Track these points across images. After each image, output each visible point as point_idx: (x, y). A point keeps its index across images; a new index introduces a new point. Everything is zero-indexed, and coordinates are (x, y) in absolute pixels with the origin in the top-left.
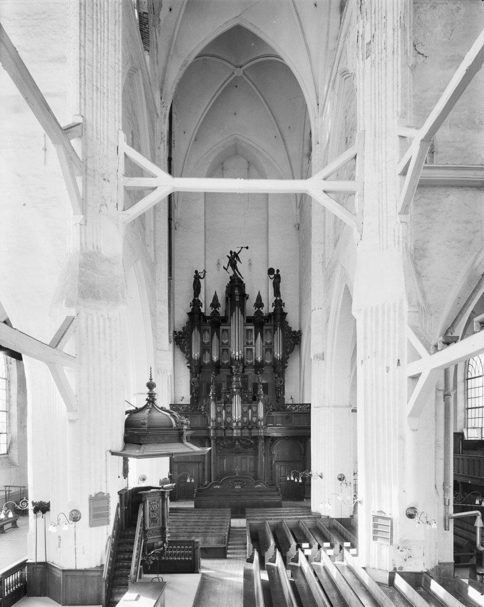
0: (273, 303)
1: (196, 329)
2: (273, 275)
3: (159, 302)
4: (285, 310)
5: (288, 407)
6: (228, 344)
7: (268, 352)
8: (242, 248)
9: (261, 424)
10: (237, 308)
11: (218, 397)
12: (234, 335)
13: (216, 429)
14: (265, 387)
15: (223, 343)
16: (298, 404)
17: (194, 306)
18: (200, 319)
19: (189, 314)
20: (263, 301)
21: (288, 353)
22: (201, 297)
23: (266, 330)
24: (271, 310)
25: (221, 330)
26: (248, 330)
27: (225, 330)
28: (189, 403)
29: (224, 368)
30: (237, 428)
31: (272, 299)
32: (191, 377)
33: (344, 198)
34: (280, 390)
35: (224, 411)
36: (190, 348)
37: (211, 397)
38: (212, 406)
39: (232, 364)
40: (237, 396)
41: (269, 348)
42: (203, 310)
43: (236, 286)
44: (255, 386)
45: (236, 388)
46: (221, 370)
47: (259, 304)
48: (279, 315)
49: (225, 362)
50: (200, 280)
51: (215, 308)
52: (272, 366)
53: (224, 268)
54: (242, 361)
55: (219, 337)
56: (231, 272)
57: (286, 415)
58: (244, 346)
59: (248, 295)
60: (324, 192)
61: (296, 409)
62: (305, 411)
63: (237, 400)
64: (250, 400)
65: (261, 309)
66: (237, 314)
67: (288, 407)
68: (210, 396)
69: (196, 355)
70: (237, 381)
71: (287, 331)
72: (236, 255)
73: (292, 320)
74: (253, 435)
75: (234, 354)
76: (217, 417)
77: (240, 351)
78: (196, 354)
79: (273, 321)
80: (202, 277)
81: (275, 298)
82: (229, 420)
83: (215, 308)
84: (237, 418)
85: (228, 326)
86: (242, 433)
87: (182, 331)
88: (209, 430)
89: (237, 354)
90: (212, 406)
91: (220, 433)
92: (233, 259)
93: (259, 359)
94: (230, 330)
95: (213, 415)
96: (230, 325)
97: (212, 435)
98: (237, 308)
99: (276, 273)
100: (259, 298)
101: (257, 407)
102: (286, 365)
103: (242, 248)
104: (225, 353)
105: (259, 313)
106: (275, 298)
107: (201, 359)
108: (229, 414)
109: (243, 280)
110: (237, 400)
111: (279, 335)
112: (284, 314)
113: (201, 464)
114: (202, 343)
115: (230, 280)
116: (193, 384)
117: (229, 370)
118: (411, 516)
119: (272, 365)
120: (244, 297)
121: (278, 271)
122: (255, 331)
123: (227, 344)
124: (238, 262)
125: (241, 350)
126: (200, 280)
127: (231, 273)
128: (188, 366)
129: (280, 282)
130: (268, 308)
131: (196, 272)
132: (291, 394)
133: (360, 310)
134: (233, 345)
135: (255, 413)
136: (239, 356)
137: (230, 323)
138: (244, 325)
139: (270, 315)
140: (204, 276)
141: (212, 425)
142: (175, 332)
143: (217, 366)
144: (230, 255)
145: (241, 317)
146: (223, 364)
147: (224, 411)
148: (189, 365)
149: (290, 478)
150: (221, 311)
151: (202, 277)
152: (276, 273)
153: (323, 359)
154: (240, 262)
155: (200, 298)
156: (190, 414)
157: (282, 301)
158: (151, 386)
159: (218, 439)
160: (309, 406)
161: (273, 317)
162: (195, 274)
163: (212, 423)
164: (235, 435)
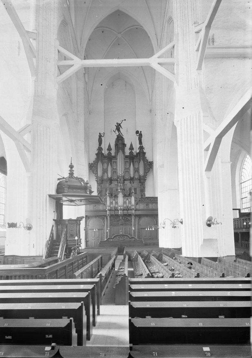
2: (139, 134)
3: (80, 141)
4: (145, 151)
6: (116, 169)
7: (137, 172)
10: (120, 150)
13: (110, 210)
14: (135, 189)
15: (114, 169)
18: (102, 156)
19: (96, 154)
20: (134, 147)
21: (146, 173)
22: (103, 146)
24: (138, 151)
25: (112, 162)
26: (126, 162)
27: (114, 162)
29: (114, 181)
30: (121, 209)
31: (138, 146)
32: (98, 186)
33: (170, 67)
34: (143, 191)
35: (114, 202)
36: (97, 171)
38: (108, 199)
39: (118, 178)
40: (120, 193)
41: (136, 170)
42: (103, 152)
43: (120, 141)
44: (130, 189)
45: (120, 189)
46: (112, 182)
47: (131, 148)
48: (142, 153)
50: (102, 137)
53: (114, 131)
54: (124, 177)
55: (111, 166)
56: (117, 133)
58: (124, 170)
60: (158, 64)
62: (155, 200)
63: (120, 196)
64: (127, 195)
65: (132, 151)
70: (121, 186)
73: (148, 157)
74: (129, 213)
78: (100, 173)
79: (139, 157)
80: (103, 136)
82: (116, 206)
83: (110, 151)
84: (121, 205)
85: (116, 160)
86: (123, 213)
87: (93, 163)
88: (106, 211)
90: (108, 199)
91: (113, 213)
95: (108, 203)
96: (117, 160)
98: (120, 150)
99: (140, 133)
100: (131, 145)
102: (146, 178)
104: (115, 173)
107: (102, 177)
108: (117, 203)
109: (123, 137)
111: (142, 164)
112: (145, 153)
114: (103, 168)
115: (117, 137)
117: (117, 182)
118: (209, 225)
119: (139, 178)
120: (124, 145)
121: (141, 132)
122: (130, 162)
123: (116, 169)
124: (121, 128)
127: (117, 133)
128: (96, 180)
130: (136, 150)
131: (100, 133)
132: (148, 194)
133: (178, 121)
134: (118, 169)
135: (130, 203)
138: (124, 159)
139: (137, 154)
142: (89, 163)
143: (111, 180)
144: (117, 125)
145: (122, 155)
147: (114, 202)
148: (96, 179)
149: (147, 229)
150: (113, 152)
151: (103, 136)
152: (140, 133)
153: (163, 167)
155: (102, 146)
158: (71, 167)
159: (111, 216)
160: (157, 198)
163: (108, 207)
164: (120, 213)
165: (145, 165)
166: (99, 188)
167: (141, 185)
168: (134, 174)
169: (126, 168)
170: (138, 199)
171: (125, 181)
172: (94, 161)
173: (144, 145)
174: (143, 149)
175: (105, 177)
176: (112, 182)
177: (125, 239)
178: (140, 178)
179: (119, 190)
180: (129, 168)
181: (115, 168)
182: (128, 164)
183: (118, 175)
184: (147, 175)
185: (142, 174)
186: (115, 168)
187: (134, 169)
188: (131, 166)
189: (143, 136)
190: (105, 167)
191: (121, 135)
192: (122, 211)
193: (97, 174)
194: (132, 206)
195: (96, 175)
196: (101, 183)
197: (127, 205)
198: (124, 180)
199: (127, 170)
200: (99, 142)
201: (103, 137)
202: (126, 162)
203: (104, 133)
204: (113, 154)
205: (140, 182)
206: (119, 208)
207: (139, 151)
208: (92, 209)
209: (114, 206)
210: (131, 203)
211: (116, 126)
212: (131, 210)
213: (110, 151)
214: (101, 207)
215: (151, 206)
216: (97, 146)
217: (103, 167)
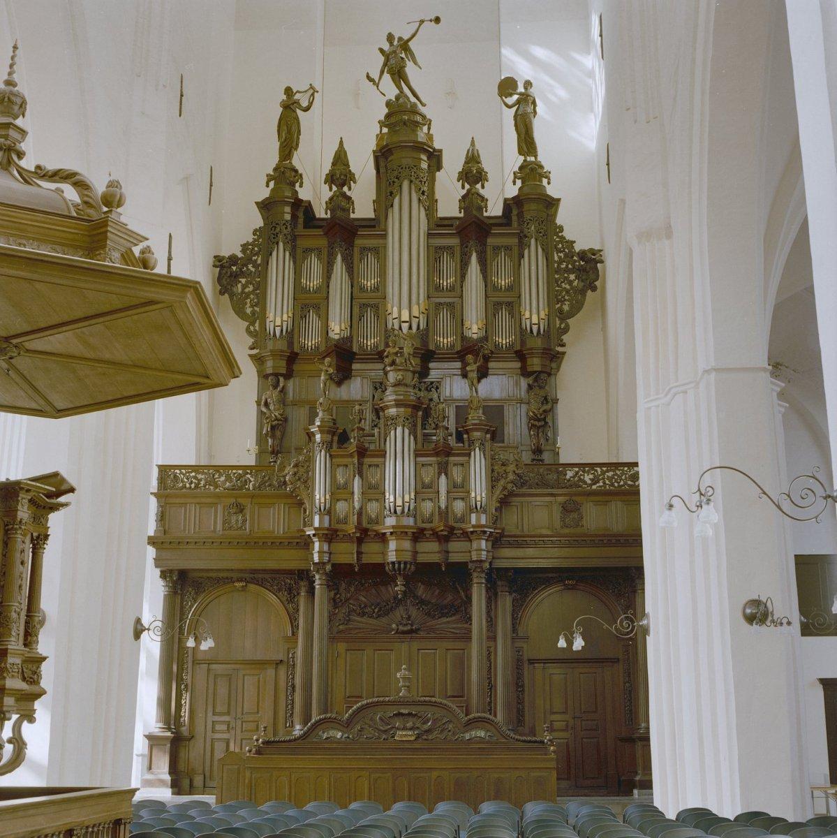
1: (281, 244)
2: (515, 97)
4: (552, 191)
5: (570, 474)
6: (380, 289)
7: (504, 314)
8: (422, 22)
9: (478, 519)
10: (406, 184)
11: (338, 437)
12: (397, 260)
13: (330, 535)
18: (294, 217)
19: (264, 206)
20: (486, 164)
21: (564, 316)
22: (299, 160)
23: (497, 249)
24: (512, 191)
25: (356, 250)
26: (440, 249)
27: (370, 249)
28: (253, 463)
30: (399, 532)
31: (514, 160)
34: (542, 422)
36: (261, 301)
37: (318, 437)
38: (320, 461)
40: (399, 430)
42: (304, 194)
45: (398, 404)
47: (473, 174)
49: (371, 342)
50: (298, 111)
52: (516, 352)
54: (424, 335)
55: (350, 270)
56: (389, 89)
57: (561, 499)
59: (441, 151)
61: (595, 481)
66: (407, 201)
67: (570, 474)
68: (313, 434)
69: (278, 322)
71: (559, 251)
74: (454, 558)
75: (395, 315)
76: (335, 498)
78: (278, 316)
80: (305, 104)
84: (399, 502)
86: (415, 553)
87: (240, 255)
88: (306, 544)
90: (320, 461)
91: (346, 554)
93: (475, 328)
94: (385, 247)
95: (320, 494)
96: (384, 236)
97: (316, 559)
99: (521, 89)
100: (473, 158)
101: (465, 466)
102: (560, 349)
103: (422, 22)
104: (369, 314)
105: (472, 202)
107: (290, 336)
108: (374, 491)
110: (399, 441)
112: (553, 204)
113: (282, 671)
114: (299, 290)
116: (264, 409)
121: (528, 84)
125: (418, 304)
126: (298, 111)
128: (250, 356)
131: (288, 91)
134: (392, 290)
135: (460, 489)
136: (410, 322)
137: (385, 230)
139: (509, 205)
140: (311, 104)
141: (317, 524)
142: (218, 259)
144: (386, 47)
146: (361, 347)
151: (305, 104)
152: (521, 89)
154: (415, 63)
156: (253, 497)
159: (339, 574)
161: (515, 212)
162: (284, 97)
163: (317, 518)
164: (392, 557)
166: (266, 404)
167: (530, 387)
168: (489, 326)
169: (438, 288)
170: (511, 468)
171: (431, 365)
172: (245, 247)
173: (546, 156)
174: (545, 181)
175: (311, 340)
176: (355, 366)
177: (428, 731)
178: (523, 343)
179: (393, 411)
180: (458, 290)
181: (370, 283)
182: (449, 266)
183: (390, 326)
184: (566, 330)
185: (535, 320)
186: (370, 283)
187: (489, 287)
190: (313, 280)
192: (407, 545)
193: (263, 317)
194: (472, 509)
195: (253, 323)
196: (284, 371)
197: (443, 506)
198: (427, 355)
201: (307, 109)
202: (435, 255)
203: (313, 91)
204: (363, 208)
206: (390, 521)
207: (520, 189)
208: (219, 527)
209: (357, 505)
210: (469, 492)
211: (381, 50)
212: (467, 536)
213: (345, 189)
214: (275, 521)
215: (594, 518)
216: (272, 159)
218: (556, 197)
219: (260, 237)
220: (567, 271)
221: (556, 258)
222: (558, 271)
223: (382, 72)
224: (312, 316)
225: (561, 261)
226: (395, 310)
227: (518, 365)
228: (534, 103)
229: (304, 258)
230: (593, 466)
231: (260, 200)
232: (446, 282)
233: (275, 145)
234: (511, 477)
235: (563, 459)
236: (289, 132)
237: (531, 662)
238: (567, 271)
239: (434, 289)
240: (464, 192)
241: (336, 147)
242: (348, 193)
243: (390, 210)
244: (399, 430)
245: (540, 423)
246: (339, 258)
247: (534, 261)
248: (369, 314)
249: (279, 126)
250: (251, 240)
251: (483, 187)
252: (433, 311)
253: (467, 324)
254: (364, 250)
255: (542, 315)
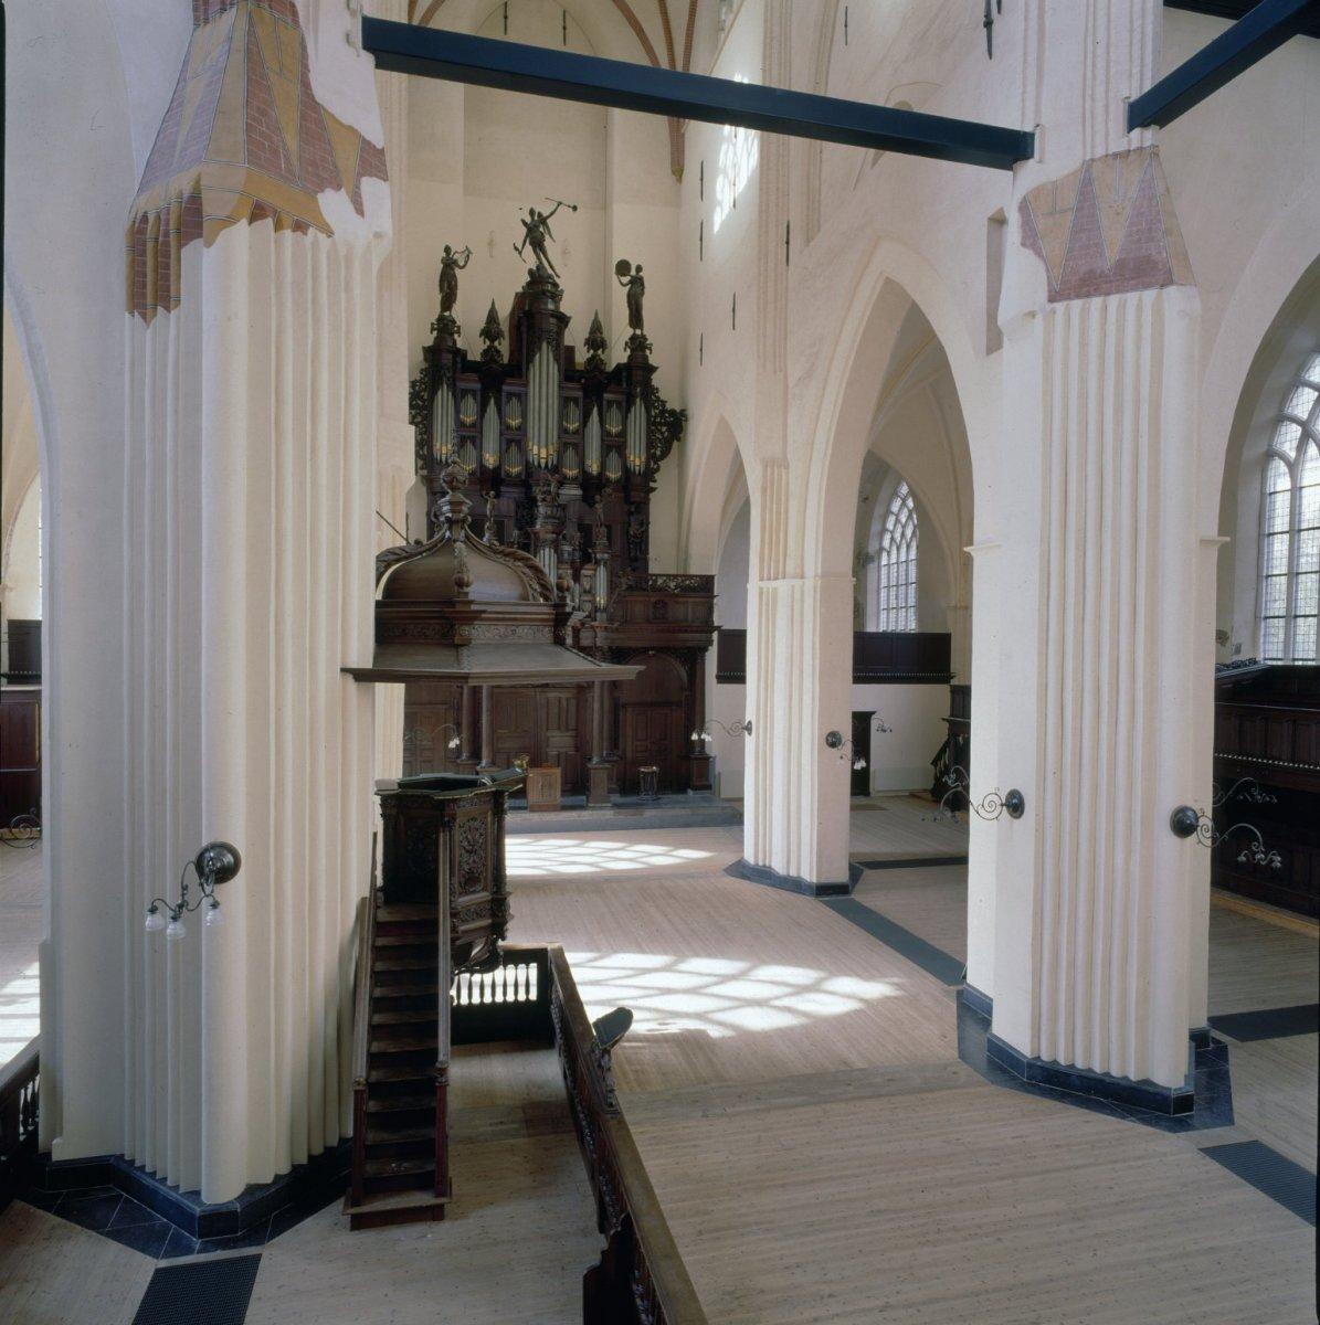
0: (626, 344)
1: (445, 386)
4: (653, 360)
5: (660, 581)
6: (522, 428)
8: (560, 204)
10: (544, 345)
15: (509, 427)
16: (681, 576)
17: (439, 330)
18: (455, 362)
21: (657, 459)
22: (458, 312)
23: (610, 403)
27: (514, 394)
40: (547, 550)
41: (614, 445)
47: (596, 341)
49: (515, 470)
50: (457, 271)
51: (492, 341)
53: (516, 249)
55: (499, 411)
65: (600, 352)
67: (660, 581)
71: (655, 408)
72: (543, 220)
77: (550, 447)
80: (462, 264)
81: (630, 332)
83: (492, 341)
89: (543, 454)
92: (536, 233)
96: (526, 385)
99: (633, 272)
100: (596, 328)
102: (652, 484)
104: (514, 448)
105: (595, 363)
106: (630, 332)
114: (460, 425)
116: (434, 519)
121: (639, 269)
124: (547, 237)
127: (532, 262)
129: (642, 294)
130: (618, 355)
131: (447, 250)
132: (661, 561)
134: (532, 431)
136: (547, 458)
140: (466, 262)
144: (528, 220)
146: (508, 475)
151: (462, 264)
152: (633, 272)
154: (551, 236)
157: (646, 339)
162: (444, 255)
165: (651, 423)
168: (603, 466)
169: (566, 431)
173: (650, 329)
174: (648, 352)
181: (514, 423)
182: (575, 412)
184: (658, 469)
185: (637, 463)
186: (514, 423)
188: (589, 424)
189: (646, 290)
190: (469, 418)
191: (550, 271)
199: (571, 442)
200: (441, 290)
202: (565, 402)
203: (468, 254)
205: (627, 500)
217: (457, 411)
218: (655, 365)
219: (425, 376)
220: (660, 424)
221: (653, 414)
222: (654, 424)
223: (525, 242)
224: (469, 445)
225: (655, 417)
226: (535, 448)
227: (623, 495)
228: (642, 284)
229: (463, 397)
230: (675, 576)
231: (426, 345)
232: (572, 427)
233: (438, 297)
234: (624, 587)
235: (650, 572)
236: (449, 287)
237: (624, 706)
238: (660, 424)
239: (563, 431)
240: (589, 355)
241: (489, 307)
242: (499, 347)
243: (531, 366)
244: (547, 550)
245: (638, 541)
246: (492, 401)
247: (638, 413)
248: (514, 448)
249: (441, 281)
250: (418, 378)
251: (603, 352)
252: (563, 446)
253: (588, 462)
254: (510, 395)
255: (643, 459)
